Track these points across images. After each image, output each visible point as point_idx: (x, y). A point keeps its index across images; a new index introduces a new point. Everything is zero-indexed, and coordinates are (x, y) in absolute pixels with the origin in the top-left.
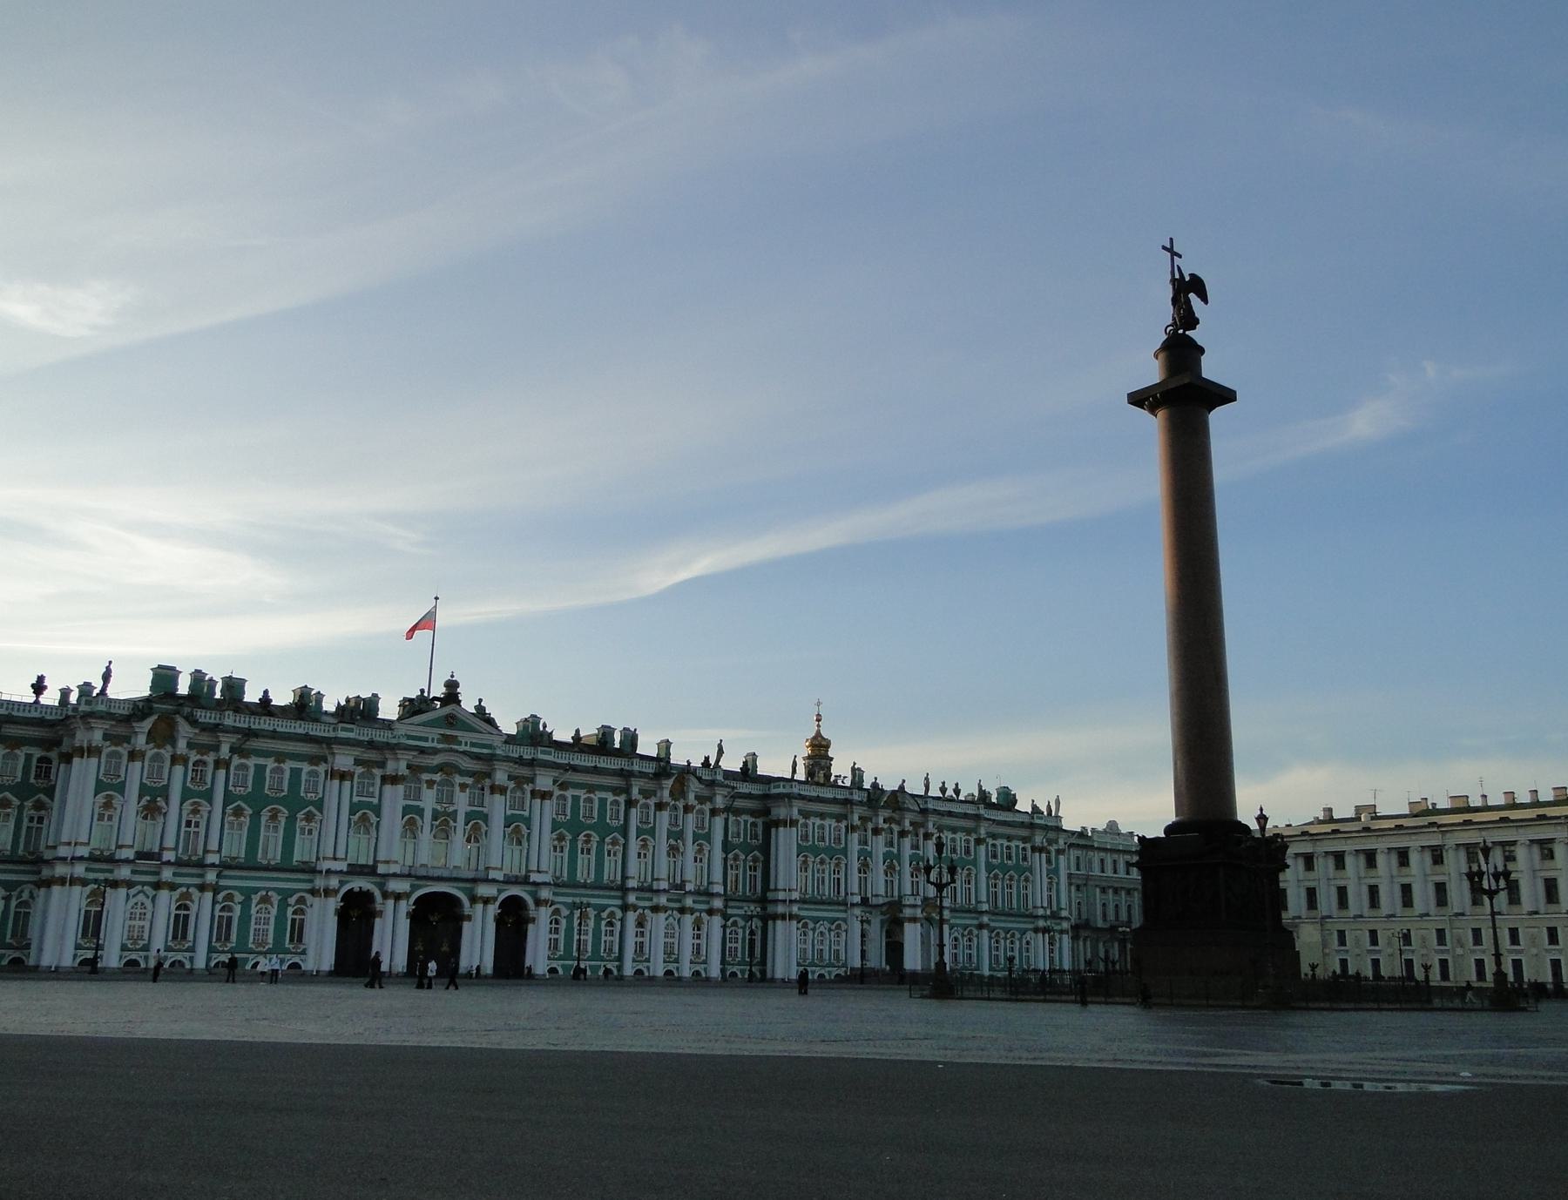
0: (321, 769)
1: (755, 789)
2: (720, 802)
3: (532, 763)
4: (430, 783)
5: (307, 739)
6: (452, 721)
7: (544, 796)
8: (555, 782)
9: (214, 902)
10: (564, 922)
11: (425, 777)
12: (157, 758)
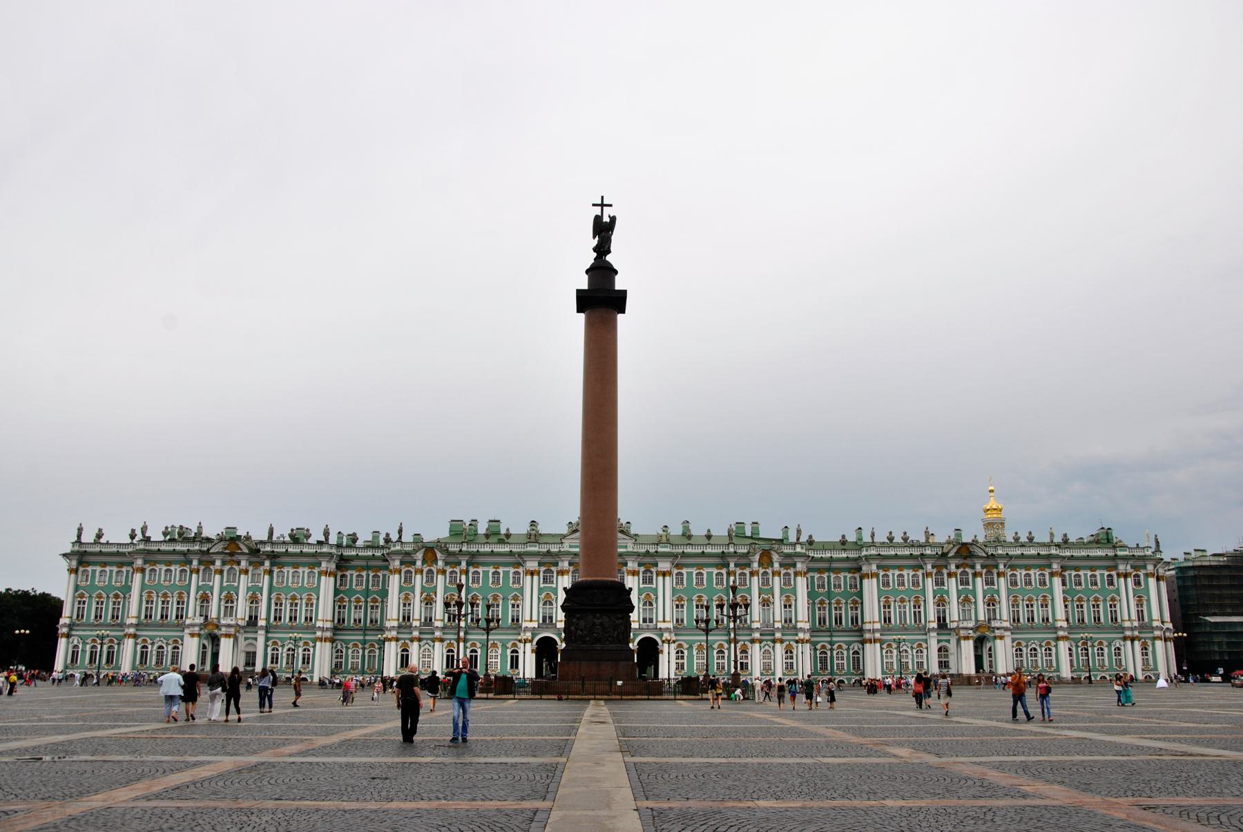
0: (521, 570)
1: (852, 555)
2: (799, 566)
5: (511, 553)
7: (664, 574)
9: (465, 648)
12: (430, 572)
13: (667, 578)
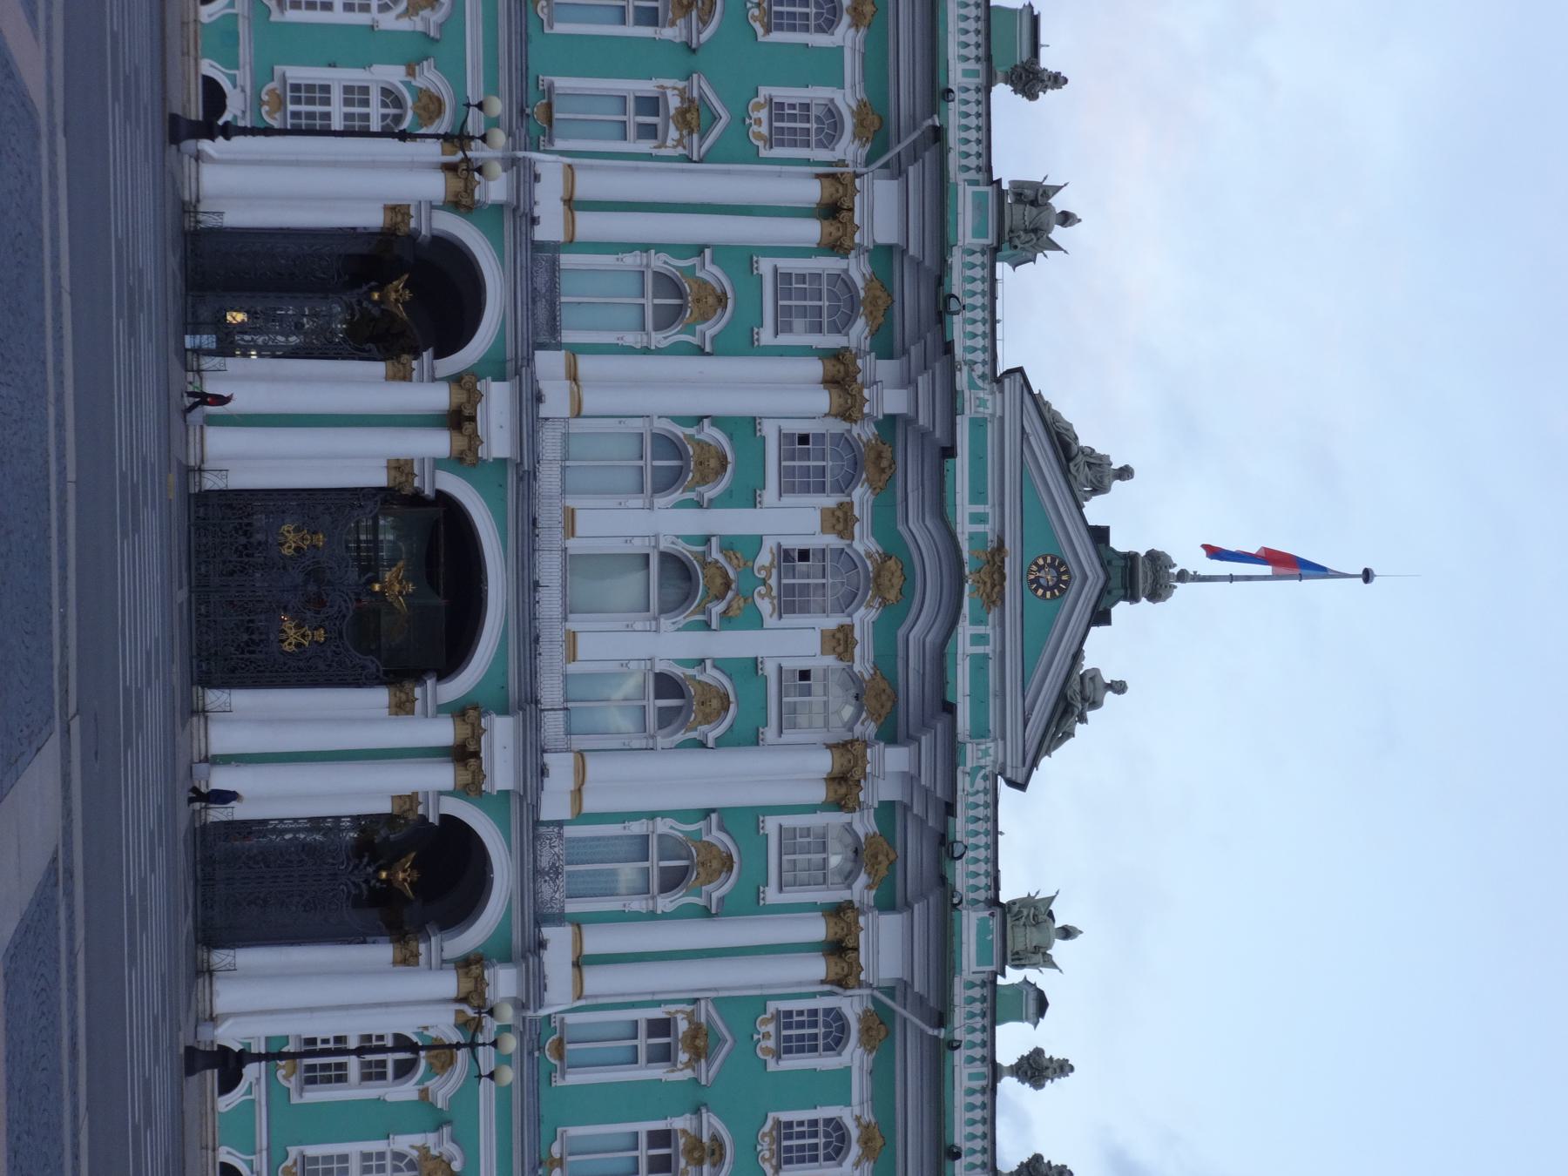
0: (848, 149)
3: (947, 905)
4: (841, 521)
6: (1053, 578)
7: (839, 949)
8: (890, 991)
10: (406, 1091)
11: (861, 495)
13: (816, 968)
